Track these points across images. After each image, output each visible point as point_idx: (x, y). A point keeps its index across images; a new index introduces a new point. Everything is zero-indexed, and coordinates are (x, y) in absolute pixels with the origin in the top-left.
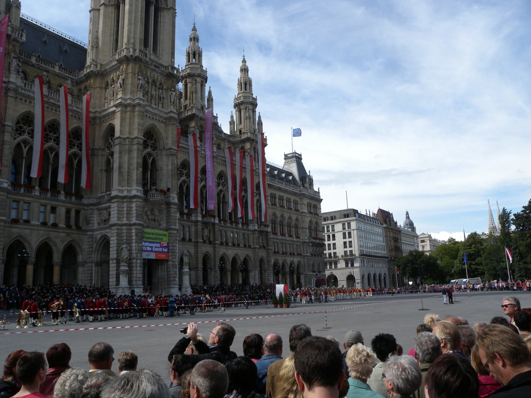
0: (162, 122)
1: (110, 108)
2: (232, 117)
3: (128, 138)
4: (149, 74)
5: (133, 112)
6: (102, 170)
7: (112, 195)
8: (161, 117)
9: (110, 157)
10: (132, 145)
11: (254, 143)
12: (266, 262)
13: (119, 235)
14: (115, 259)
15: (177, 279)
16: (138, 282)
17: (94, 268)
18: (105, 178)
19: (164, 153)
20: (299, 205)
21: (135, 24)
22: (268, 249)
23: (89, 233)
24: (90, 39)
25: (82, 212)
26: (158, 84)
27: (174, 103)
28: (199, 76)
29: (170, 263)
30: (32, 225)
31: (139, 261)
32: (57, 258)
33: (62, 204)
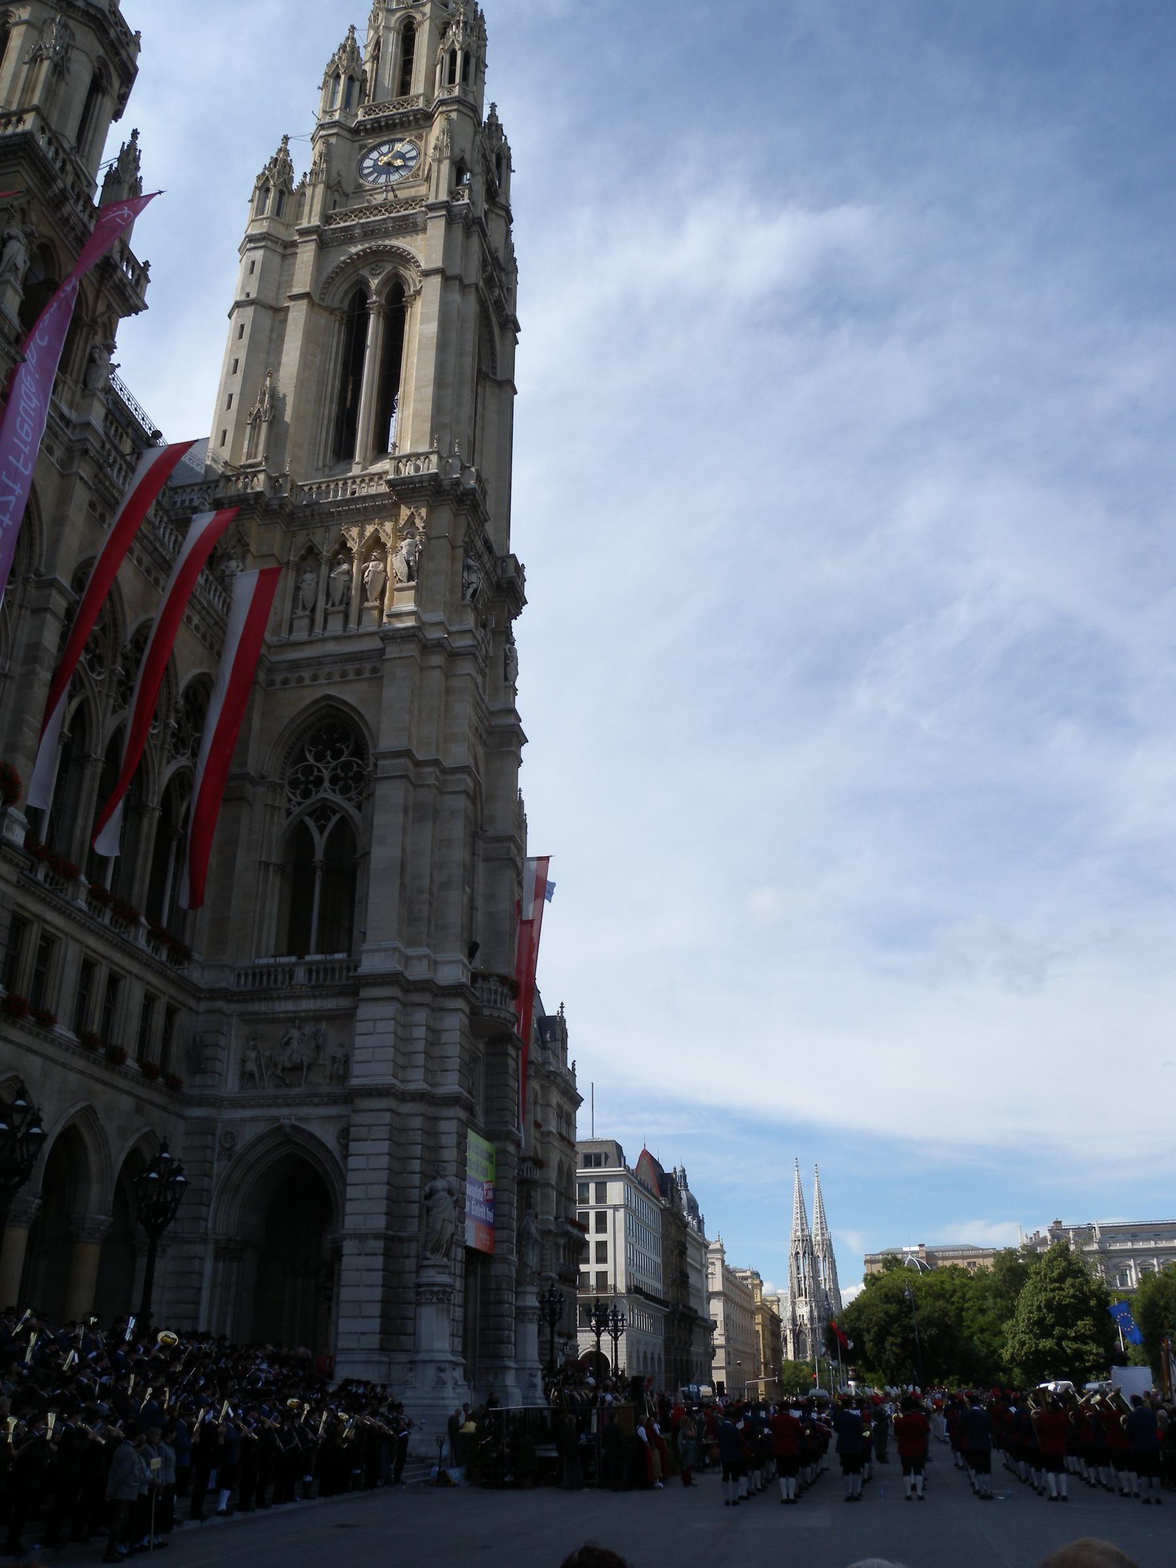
1: (324, 640)
3: (436, 763)
5: (448, 674)
6: (267, 865)
7: (360, 971)
9: (310, 823)
10: (441, 793)
13: (397, 1136)
14: (376, 1237)
17: (208, 1266)
18: (277, 896)
23: (197, 1112)
24: (236, 390)
25: (182, 1018)
29: (498, 1269)
30: (53, 1042)
32: (96, 1200)
33: (134, 967)
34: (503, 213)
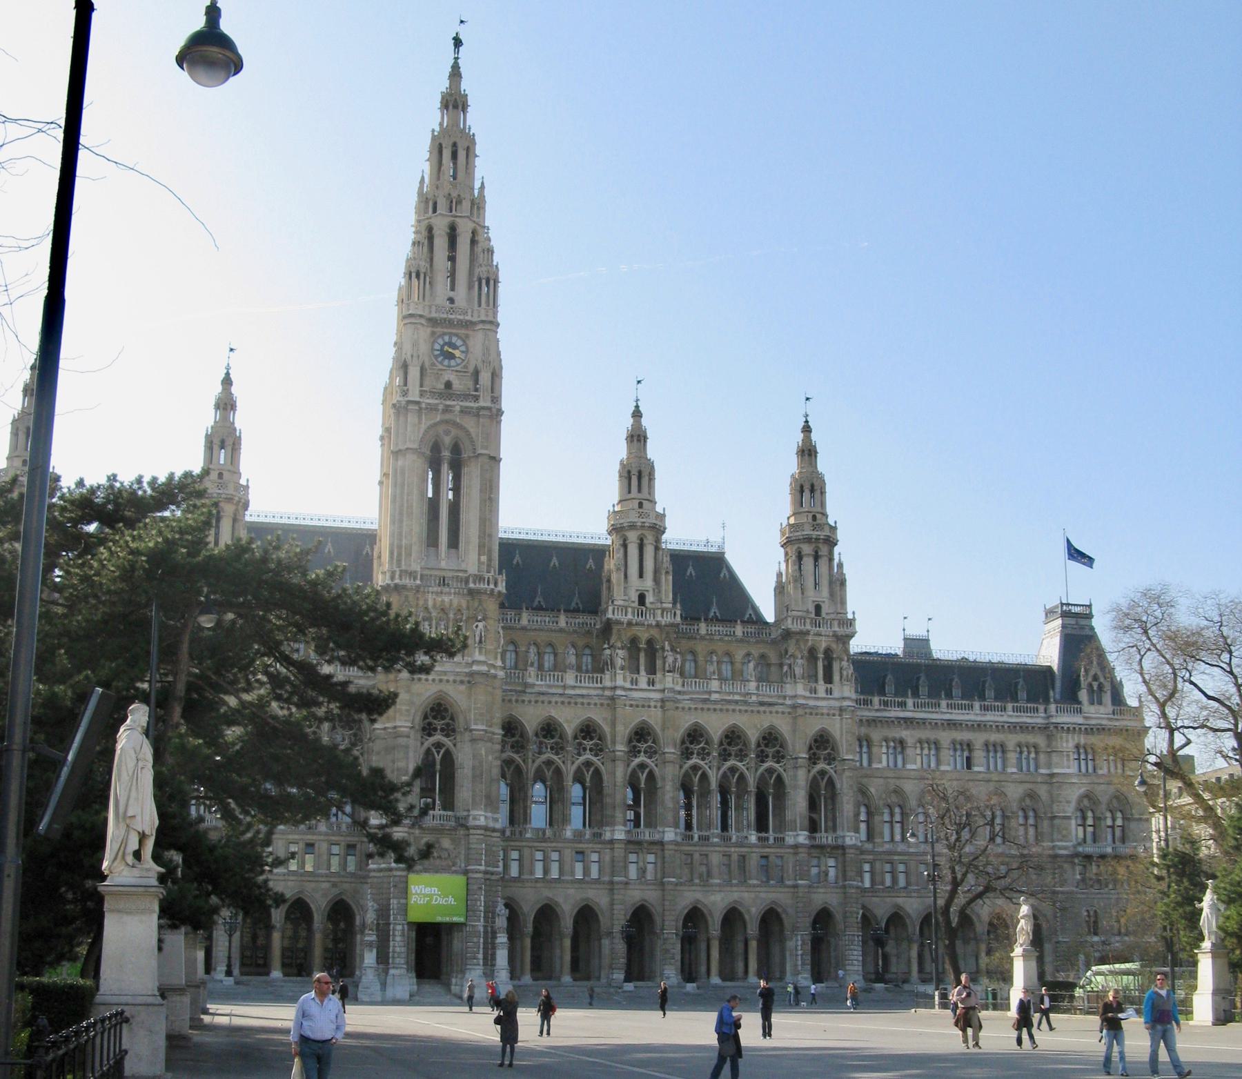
0: (462, 682)
2: (779, 575)
4: (430, 603)
8: (458, 674)
11: (810, 638)
12: (838, 917)
15: (481, 956)
16: (397, 960)
19: (467, 736)
20: (1042, 757)
21: (401, 521)
22: (844, 887)
26: (451, 616)
27: (480, 642)
28: (632, 527)
31: (399, 927)
34: (480, 326)
